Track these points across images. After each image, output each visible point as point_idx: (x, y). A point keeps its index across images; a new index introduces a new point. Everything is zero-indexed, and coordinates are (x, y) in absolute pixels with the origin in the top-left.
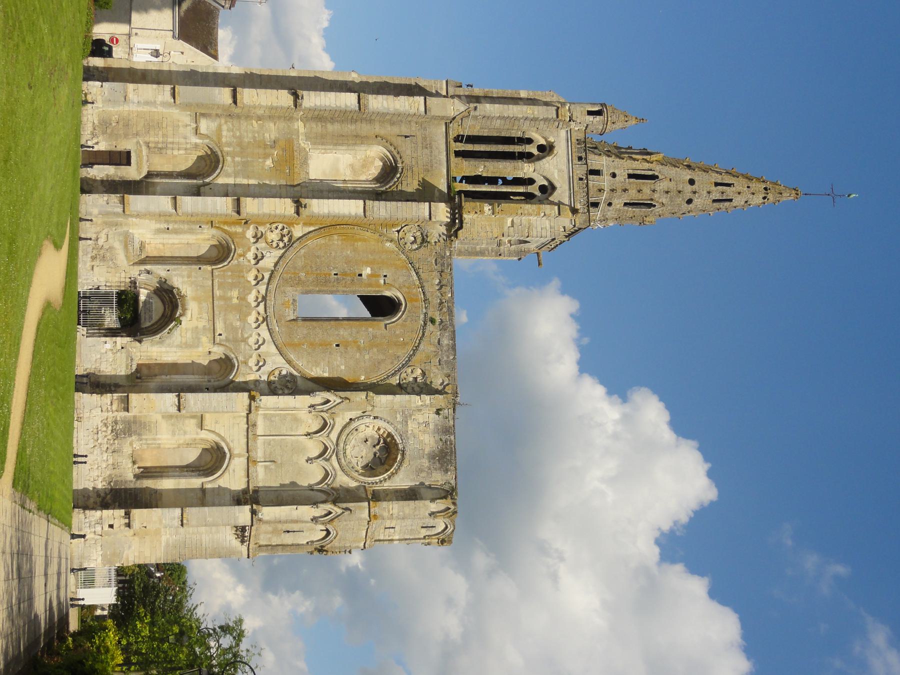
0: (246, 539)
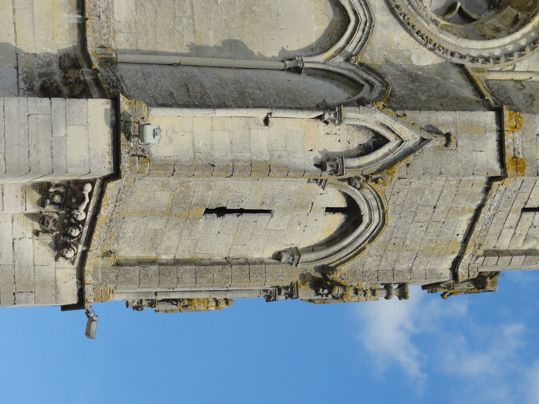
0: (75, 233)
